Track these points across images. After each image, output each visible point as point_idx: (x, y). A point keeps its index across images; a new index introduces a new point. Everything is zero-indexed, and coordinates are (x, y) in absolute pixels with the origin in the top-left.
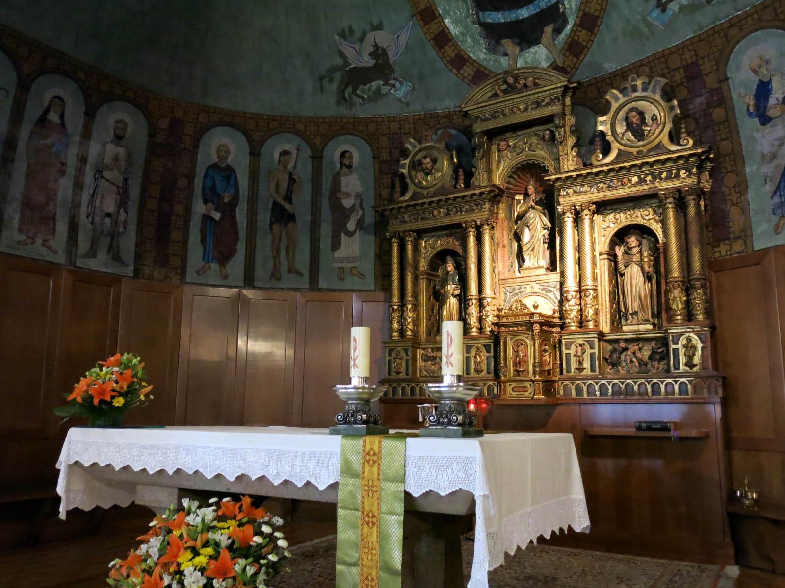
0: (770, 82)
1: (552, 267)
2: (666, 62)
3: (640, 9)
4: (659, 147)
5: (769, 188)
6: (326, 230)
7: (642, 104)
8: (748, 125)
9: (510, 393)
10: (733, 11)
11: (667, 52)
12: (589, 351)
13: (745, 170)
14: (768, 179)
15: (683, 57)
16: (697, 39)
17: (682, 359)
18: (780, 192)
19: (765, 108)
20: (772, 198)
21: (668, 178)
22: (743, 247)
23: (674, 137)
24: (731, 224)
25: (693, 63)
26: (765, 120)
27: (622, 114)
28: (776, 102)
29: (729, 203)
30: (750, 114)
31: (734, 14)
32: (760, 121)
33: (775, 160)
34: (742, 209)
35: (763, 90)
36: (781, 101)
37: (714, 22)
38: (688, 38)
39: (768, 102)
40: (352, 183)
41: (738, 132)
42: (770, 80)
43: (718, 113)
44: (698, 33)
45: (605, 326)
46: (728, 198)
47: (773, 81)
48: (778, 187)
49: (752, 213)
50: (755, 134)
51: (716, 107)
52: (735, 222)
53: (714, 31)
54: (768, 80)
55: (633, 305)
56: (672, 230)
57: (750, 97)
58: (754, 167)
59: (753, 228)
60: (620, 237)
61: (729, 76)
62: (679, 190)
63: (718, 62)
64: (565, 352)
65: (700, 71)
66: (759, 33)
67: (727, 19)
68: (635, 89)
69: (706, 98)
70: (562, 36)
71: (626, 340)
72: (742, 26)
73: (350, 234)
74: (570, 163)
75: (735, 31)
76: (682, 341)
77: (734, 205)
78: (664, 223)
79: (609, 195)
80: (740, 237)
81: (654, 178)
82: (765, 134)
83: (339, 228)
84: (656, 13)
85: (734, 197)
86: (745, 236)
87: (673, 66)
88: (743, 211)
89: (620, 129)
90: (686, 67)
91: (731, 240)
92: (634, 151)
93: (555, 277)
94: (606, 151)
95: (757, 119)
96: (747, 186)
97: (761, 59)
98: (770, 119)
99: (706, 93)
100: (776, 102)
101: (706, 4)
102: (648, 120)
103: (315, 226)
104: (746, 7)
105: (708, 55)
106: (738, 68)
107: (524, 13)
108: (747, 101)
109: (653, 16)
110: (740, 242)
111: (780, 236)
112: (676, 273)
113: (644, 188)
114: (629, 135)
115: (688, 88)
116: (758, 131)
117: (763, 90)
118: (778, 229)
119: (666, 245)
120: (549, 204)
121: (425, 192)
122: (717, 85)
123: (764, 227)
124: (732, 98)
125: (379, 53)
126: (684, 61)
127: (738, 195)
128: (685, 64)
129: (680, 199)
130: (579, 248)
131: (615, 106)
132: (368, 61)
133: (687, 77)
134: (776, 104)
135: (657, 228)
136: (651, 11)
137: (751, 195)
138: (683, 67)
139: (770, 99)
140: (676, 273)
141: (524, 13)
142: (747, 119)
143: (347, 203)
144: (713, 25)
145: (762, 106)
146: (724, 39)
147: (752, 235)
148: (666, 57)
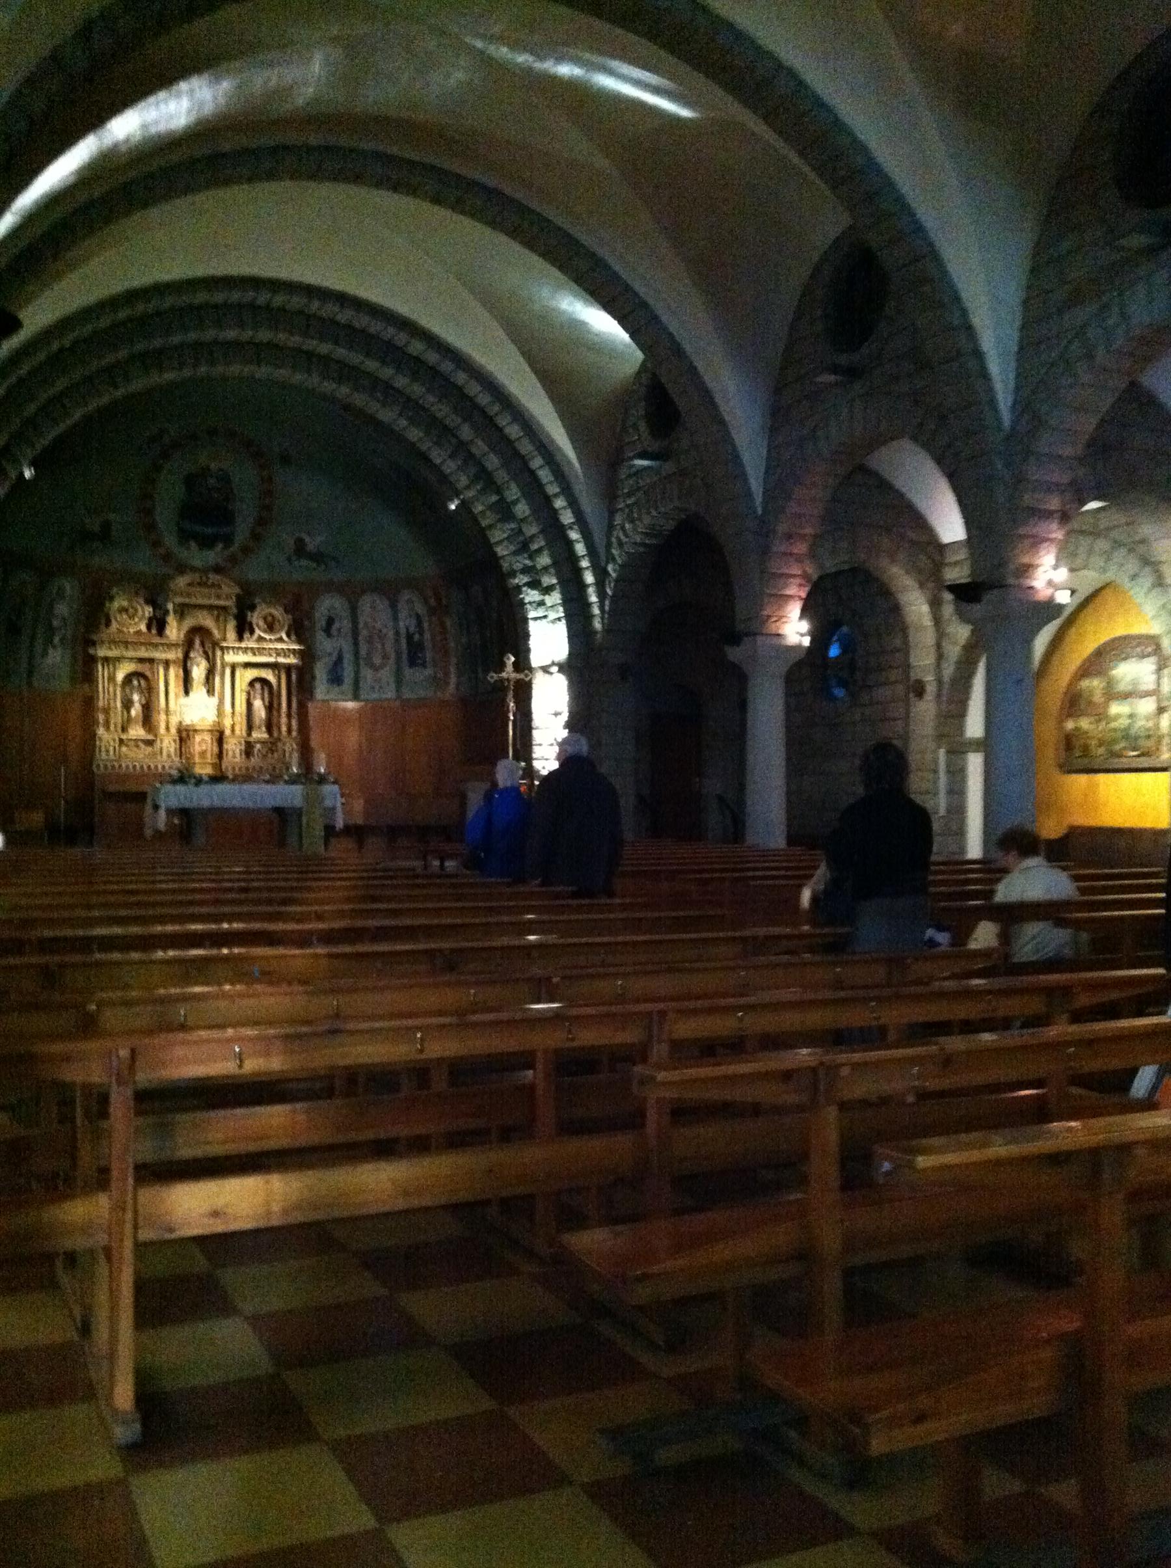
6: (39, 641)
8: (320, 636)
23: (288, 635)
35: (330, 621)
40: (62, 609)
60: (251, 684)
73: (54, 647)
74: (231, 635)
83: (49, 642)
93: (214, 701)
94: (252, 632)
103: (33, 638)
107: (209, 531)
117: (330, 621)
125: (106, 526)
129: (288, 668)
132: (97, 528)
143: (55, 623)
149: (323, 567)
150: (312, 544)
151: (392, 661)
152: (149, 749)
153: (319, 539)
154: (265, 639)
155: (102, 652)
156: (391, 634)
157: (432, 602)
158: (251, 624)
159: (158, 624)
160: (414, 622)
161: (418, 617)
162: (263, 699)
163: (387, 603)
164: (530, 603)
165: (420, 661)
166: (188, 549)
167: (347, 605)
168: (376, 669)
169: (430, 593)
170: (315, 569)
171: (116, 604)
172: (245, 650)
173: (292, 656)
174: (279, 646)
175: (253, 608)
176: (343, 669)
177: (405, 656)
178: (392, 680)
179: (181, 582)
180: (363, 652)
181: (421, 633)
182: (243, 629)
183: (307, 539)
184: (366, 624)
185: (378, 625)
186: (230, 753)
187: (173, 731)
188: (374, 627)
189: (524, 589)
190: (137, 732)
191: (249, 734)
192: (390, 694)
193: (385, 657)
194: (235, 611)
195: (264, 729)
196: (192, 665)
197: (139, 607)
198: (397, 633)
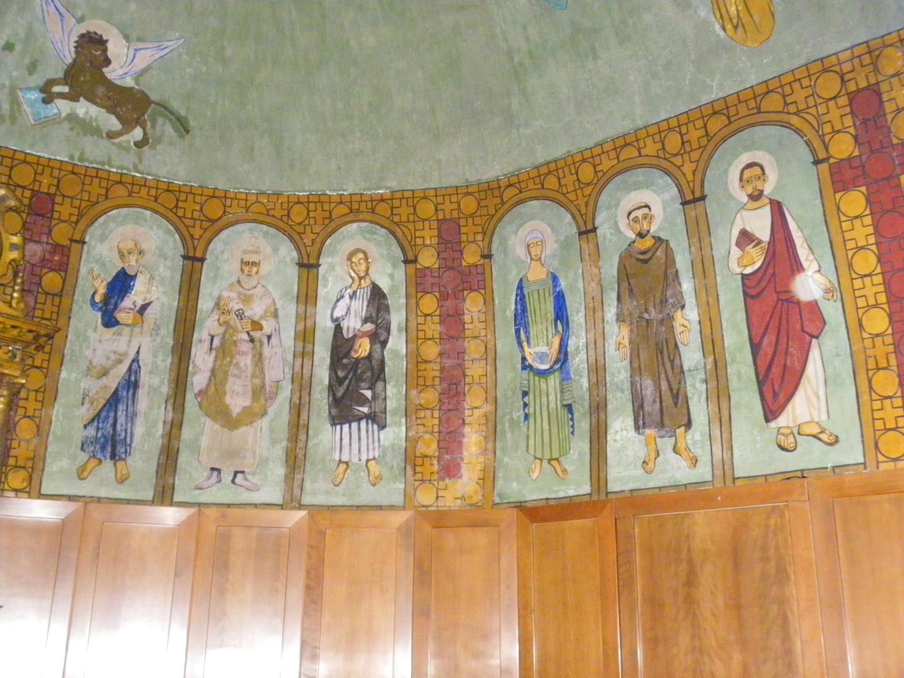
0: (133, 278)
2: (12, 168)
3: (15, 74)
5: (85, 412)
10: (131, 167)
11: (22, 157)
13: (59, 374)
14: (87, 398)
15: (38, 178)
16: (70, 168)
18: (98, 423)
19: (116, 306)
20: (85, 426)
22: (25, 484)
24: (15, 444)
25: (48, 194)
26: (110, 321)
28: (133, 307)
29: (21, 411)
30: (93, 303)
31: (130, 171)
32: (103, 319)
33: (104, 378)
34: (38, 427)
36: (137, 308)
37: (103, 164)
38: (59, 158)
39: (122, 301)
41: (70, 318)
42: (136, 274)
43: (52, 280)
44: (76, 162)
46: (21, 403)
47: (137, 278)
48: (98, 415)
49: (51, 438)
50: (90, 332)
51: (52, 270)
52: (22, 443)
53: (97, 174)
54: (133, 274)
57: (102, 281)
58: (74, 375)
59: (48, 460)
61: (87, 239)
63: (80, 215)
65: (52, 210)
66: (148, 213)
67: (119, 171)
69: (44, 250)
72: (132, 192)
75: (120, 191)
77: (28, 417)
80: (24, 468)
82: (103, 340)
84: (35, 95)
85: (32, 406)
86: (32, 468)
87: (17, 179)
88: (38, 430)
90: (34, 193)
91: (9, 468)
95: (99, 314)
96: (56, 398)
97: (136, 244)
98: (117, 323)
99: (47, 243)
100: (133, 307)
101: (104, 135)
104: (149, 174)
105: (72, 198)
106: (103, 238)
108: (97, 286)
109: (28, 96)
110: (23, 474)
111: (84, 483)
115: (24, 224)
116: (95, 330)
118: (83, 472)
122: (67, 243)
123: (64, 463)
124: (78, 271)
126: (37, 184)
127: (39, 405)
128: (36, 188)
133: (30, 206)
134: (130, 309)
136: (30, 89)
137: (57, 412)
138: (32, 190)
139: (126, 299)
142: (87, 307)
144: (100, 167)
145: (113, 301)
146: (103, 192)
147: (43, 471)
148: (16, 162)
149: (138, 133)
151: (280, 409)
153: (144, 58)
156: (288, 337)
157: (428, 259)
160: (360, 306)
161: (377, 295)
163: (287, 252)
165: (365, 410)
167: (173, 246)
168: (229, 421)
169: (429, 236)
170: (111, 135)
176: (132, 417)
177: (321, 399)
178: (279, 451)
180: (198, 380)
181: (379, 337)
183: (116, 47)
184: (219, 305)
185: (256, 310)
188: (240, 315)
192: (272, 493)
193: (258, 392)
198: (306, 336)
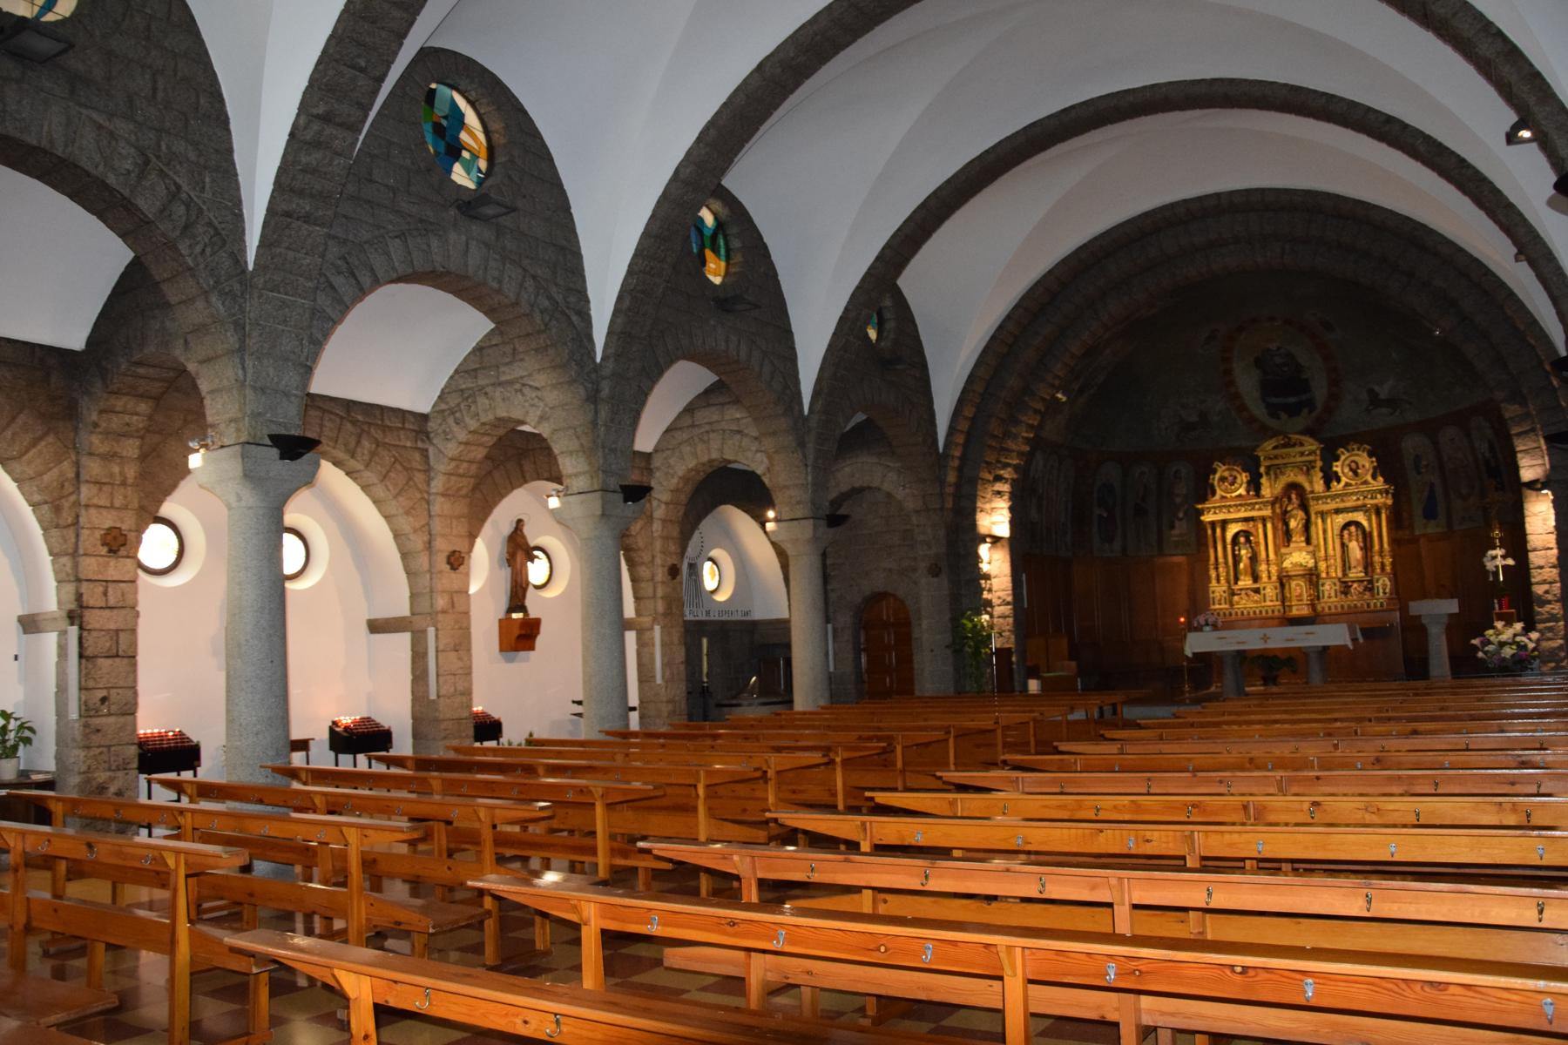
1: (1308, 541)
4: (1366, 483)
7: (1356, 458)
9: (1295, 612)
12: (1334, 588)
17: (1381, 591)
21: (1372, 498)
23: (1374, 477)
27: (1347, 462)
45: (1340, 575)
55: (1353, 563)
56: (1374, 525)
62: (1376, 505)
64: (1321, 588)
68: (1353, 450)
70: (1314, 414)
71: (1353, 582)
74: (1319, 486)
76: (1381, 582)
78: (1370, 520)
79: (1342, 505)
81: (1365, 497)
89: (1346, 470)
92: (1353, 482)
94: (1339, 481)
102: (1360, 466)
107: (1292, 400)
112: (1377, 547)
113: (1360, 503)
114: (1351, 473)
117: (1418, 458)
119: (1371, 533)
120: (1304, 507)
121: (1228, 495)
130: (1325, 531)
131: (1343, 458)
132: (1194, 418)
135: (1365, 523)
140: (1377, 547)
141: (1292, 400)
150: (1384, 392)
152: (1256, 597)
154: (1351, 485)
155: (1207, 518)
158: (1336, 473)
159: (1255, 485)
162: (1357, 540)
164: (1511, 418)
166: (1278, 418)
171: (1217, 476)
172: (1333, 497)
173: (1379, 496)
174: (1363, 488)
175: (1337, 459)
179: (1269, 445)
182: (1330, 477)
183: (1377, 388)
186: (1326, 594)
187: (1274, 578)
189: (1502, 405)
190: (1245, 582)
191: (1345, 574)
194: (1319, 464)
195: (1360, 569)
196: (1289, 518)
197: (1238, 476)
